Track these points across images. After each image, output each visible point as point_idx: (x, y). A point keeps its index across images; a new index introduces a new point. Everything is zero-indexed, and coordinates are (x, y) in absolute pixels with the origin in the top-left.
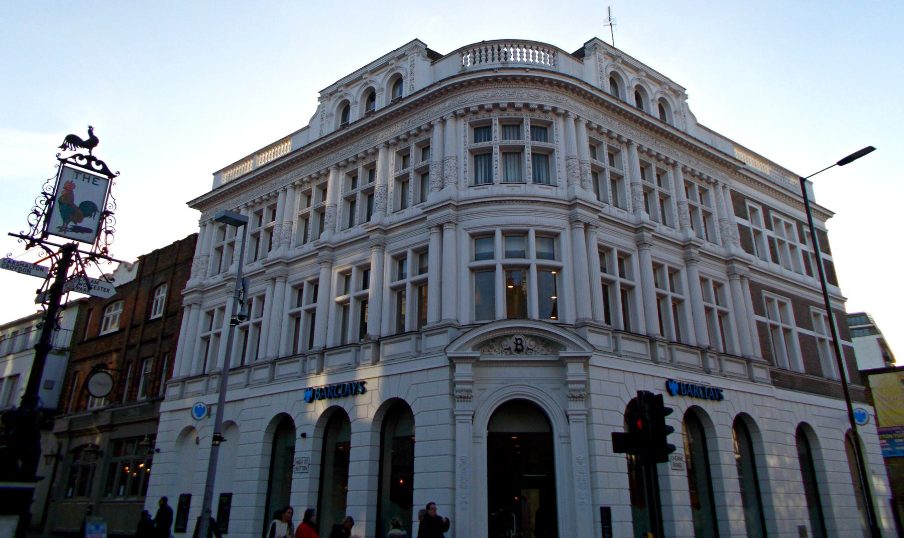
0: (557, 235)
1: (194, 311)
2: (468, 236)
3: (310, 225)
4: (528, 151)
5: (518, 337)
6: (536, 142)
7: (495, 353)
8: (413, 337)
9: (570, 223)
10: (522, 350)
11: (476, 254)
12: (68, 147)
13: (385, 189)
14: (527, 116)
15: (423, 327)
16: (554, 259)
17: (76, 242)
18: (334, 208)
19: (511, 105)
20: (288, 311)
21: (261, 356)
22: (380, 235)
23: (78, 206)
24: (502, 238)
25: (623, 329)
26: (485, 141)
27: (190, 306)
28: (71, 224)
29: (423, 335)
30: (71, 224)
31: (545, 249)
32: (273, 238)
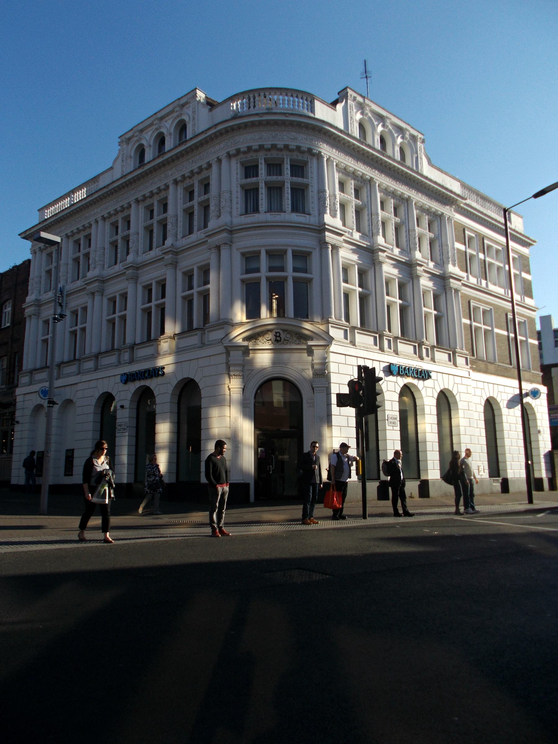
0: (309, 254)
1: (34, 321)
3: (119, 250)
4: (288, 186)
5: (277, 331)
6: (294, 178)
7: (260, 343)
8: (199, 333)
9: (320, 244)
10: (280, 341)
11: (246, 269)
13: (176, 219)
14: (287, 156)
15: (206, 325)
16: (307, 273)
19: (274, 147)
20: (105, 317)
21: (87, 352)
22: (172, 256)
24: (266, 257)
25: (359, 326)
26: (253, 177)
27: (30, 316)
29: (206, 330)
31: (299, 265)
32: (90, 261)
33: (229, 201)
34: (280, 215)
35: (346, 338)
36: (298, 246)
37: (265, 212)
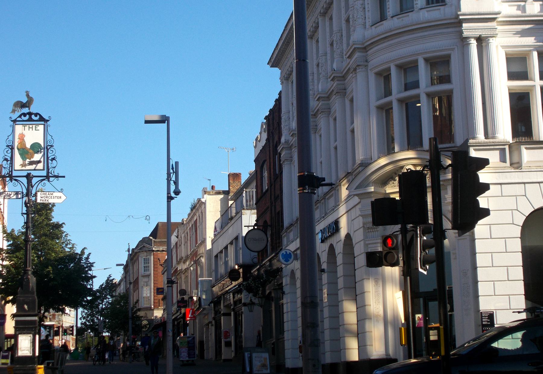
0: (449, 56)
2: (373, 75)
12: (16, 110)
27: (284, 162)
28: (28, 160)
30: (28, 160)
33: (361, 9)
35: (503, 159)
36: (429, 52)
37: (392, 17)
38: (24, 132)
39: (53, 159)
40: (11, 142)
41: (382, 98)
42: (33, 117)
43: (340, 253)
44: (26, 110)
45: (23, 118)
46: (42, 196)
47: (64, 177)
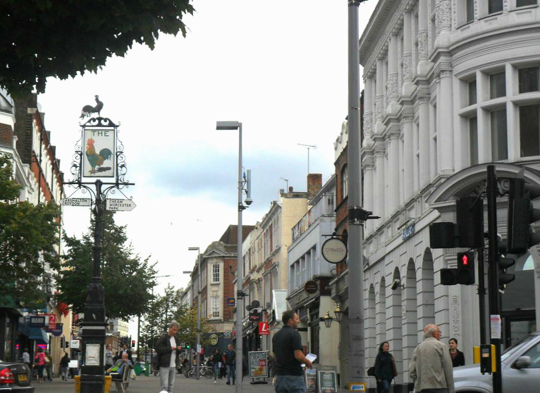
2: (458, 81)
12: (85, 115)
17: (98, 178)
18: (409, 58)
23: (98, 154)
33: (447, 10)
34: (496, 18)
37: (479, 20)
38: (94, 138)
39: (123, 166)
40: (80, 147)
41: (466, 106)
42: (103, 122)
43: (420, 268)
44: (95, 115)
45: (93, 123)
46: (111, 203)
47: (134, 184)
